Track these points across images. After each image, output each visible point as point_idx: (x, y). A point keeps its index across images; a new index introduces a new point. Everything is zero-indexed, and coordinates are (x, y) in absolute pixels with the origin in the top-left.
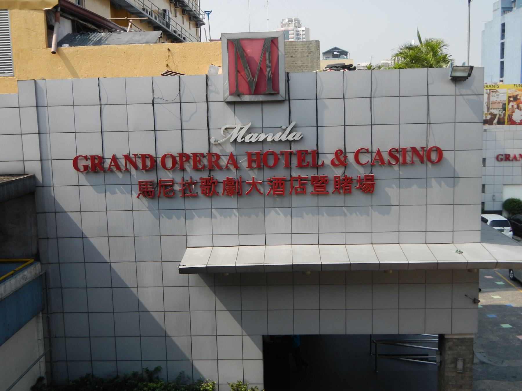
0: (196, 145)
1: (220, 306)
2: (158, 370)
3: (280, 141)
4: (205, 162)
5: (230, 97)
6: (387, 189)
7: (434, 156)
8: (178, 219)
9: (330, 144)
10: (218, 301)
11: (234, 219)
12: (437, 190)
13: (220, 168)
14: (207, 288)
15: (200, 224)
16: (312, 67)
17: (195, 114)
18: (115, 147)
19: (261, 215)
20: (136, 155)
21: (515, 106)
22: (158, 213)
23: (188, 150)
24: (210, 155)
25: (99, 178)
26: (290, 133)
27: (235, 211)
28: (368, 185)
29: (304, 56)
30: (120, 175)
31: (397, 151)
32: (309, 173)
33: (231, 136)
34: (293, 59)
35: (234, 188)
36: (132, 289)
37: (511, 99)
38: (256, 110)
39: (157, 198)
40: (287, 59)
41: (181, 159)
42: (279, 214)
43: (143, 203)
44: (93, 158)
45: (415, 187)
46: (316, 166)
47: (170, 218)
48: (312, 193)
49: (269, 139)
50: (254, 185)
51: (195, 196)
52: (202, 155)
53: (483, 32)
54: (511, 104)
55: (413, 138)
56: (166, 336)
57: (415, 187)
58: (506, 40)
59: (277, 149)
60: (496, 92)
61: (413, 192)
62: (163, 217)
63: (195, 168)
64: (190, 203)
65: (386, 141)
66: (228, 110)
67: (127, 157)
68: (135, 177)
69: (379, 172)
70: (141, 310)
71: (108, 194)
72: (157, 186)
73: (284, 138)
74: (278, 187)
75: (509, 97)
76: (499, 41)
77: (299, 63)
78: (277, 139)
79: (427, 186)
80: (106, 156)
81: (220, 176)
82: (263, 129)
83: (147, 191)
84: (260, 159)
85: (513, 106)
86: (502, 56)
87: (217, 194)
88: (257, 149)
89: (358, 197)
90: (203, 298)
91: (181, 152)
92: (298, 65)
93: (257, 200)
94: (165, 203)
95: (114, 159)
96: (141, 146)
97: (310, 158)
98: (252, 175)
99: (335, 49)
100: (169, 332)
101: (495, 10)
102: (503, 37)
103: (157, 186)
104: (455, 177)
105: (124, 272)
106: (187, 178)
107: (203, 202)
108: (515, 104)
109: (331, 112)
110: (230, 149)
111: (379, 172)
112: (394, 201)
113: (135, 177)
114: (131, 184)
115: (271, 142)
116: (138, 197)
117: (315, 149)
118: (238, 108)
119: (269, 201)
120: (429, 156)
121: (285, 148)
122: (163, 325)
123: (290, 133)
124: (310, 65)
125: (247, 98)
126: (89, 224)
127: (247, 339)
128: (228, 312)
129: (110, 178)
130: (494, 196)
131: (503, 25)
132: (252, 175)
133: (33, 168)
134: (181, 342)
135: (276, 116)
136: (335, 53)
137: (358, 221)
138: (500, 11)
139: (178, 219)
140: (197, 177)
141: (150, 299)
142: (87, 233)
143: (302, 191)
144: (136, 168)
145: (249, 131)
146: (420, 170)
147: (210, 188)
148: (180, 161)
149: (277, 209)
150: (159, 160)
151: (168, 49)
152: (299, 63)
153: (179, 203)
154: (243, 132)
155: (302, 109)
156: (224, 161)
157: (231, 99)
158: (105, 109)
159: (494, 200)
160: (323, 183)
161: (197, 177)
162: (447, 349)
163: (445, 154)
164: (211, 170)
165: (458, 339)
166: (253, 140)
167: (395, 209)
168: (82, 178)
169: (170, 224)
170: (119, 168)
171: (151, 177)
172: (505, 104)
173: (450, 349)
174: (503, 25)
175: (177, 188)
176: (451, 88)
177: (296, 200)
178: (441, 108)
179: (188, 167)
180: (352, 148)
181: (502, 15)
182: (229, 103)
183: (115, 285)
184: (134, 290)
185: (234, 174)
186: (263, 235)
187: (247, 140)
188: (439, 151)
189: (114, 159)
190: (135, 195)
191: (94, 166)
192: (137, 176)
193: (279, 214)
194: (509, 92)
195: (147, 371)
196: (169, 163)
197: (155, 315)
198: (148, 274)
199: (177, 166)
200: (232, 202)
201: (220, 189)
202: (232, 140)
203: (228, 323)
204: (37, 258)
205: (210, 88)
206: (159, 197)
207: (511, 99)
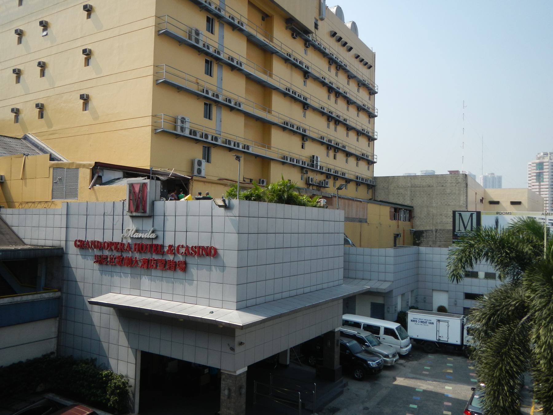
2: (96, 359)
3: (146, 238)
6: (192, 270)
7: (213, 252)
9: (169, 241)
12: (216, 273)
16: (459, 194)
19: (139, 278)
22: (102, 272)
24: (121, 244)
28: (183, 267)
29: (453, 186)
31: (195, 247)
34: (443, 188)
40: (439, 188)
43: (96, 266)
45: (205, 270)
46: (163, 254)
56: (100, 341)
57: (205, 270)
61: (204, 272)
65: (192, 242)
69: (190, 260)
70: (92, 325)
74: (148, 265)
77: (448, 191)
79: (210, 270)
84: (141, 247)
88: (138, 242)
89: (180, 274)
90: (114, 322)
92: (448, 192)
93: (138, 270)
97: (159, 249)
100: (102, 339)
104: (224, 267)
109: (170, 225)
111: (190, 260)
112: (195, 278)
120: (209, 252)
121: (149, 243)
124: (457, 192)
126: (78, 274)
127: (130, 349)
130: (456, 301)
133: (63, 244)
134: (105, 345)
135: (147, 225)
137: (179, 287)
146: (208, 260)
148: (111, 245)
152: (448, 191)
158: (88, 216)
163: (219, 251)
167: (195, 282)
169: (106, 278)
177: (154, 272)
178: (218, 224)
186: (137, 288)
188: (215, 250)
191: (82, 245)
192: (97, 252)
195: (92, 359)
197: (97, 328)
204: (60, 290)
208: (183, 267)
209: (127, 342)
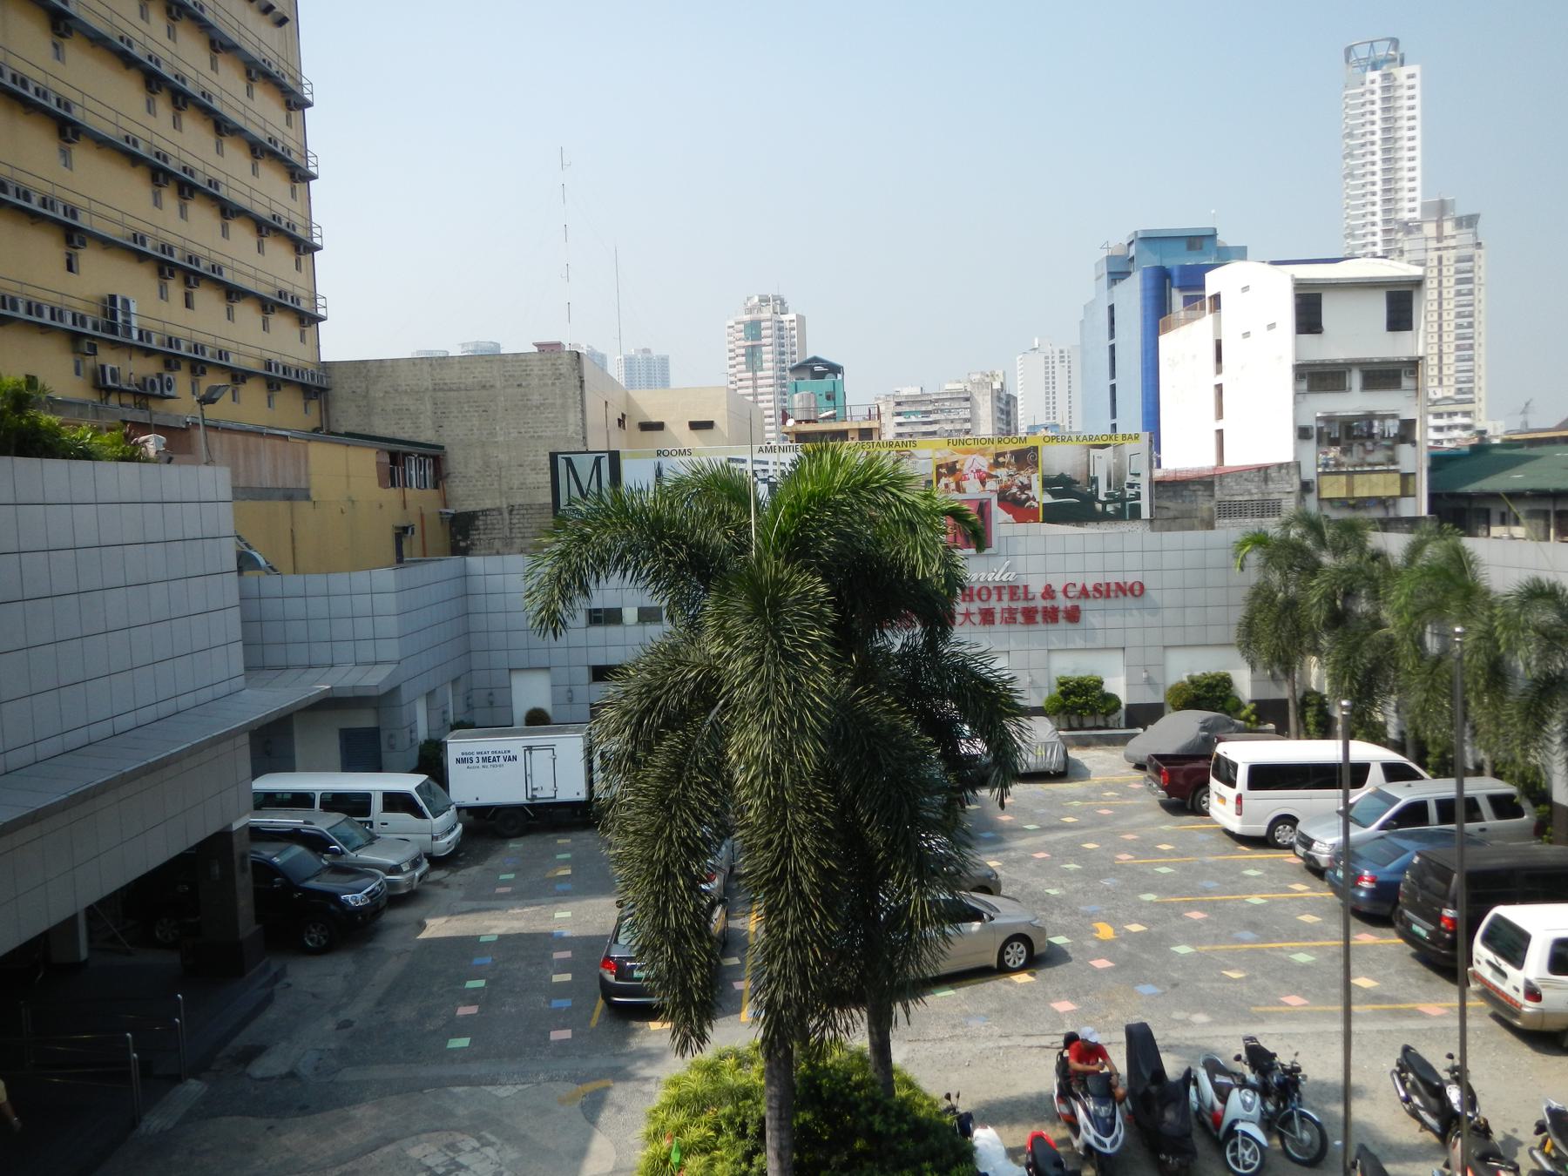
16: (563, 406)
21: (953, 486)
37: (943, 470)
53: (1082, 322)
54: (944, 481)
58: (1117, 341)
60: (911, 455)
75: (939, 467)
76: (1107, 343)
77: (536, 399)
85: (947, 486)
86: (1113, 376)
99: (816, 360)
101: (1098, 278)
102: (1112, 336)
108: (951, 481)
124: (559, 402)
131: (1112, 308)
136: (817, 369)
138: (1105, 278)
152: (536, 399)
159: (571, 700)
172: (931, 482)
174: (1112, 308)
181: (1110, 287)
194: (938, 455)
207: (943, 470)
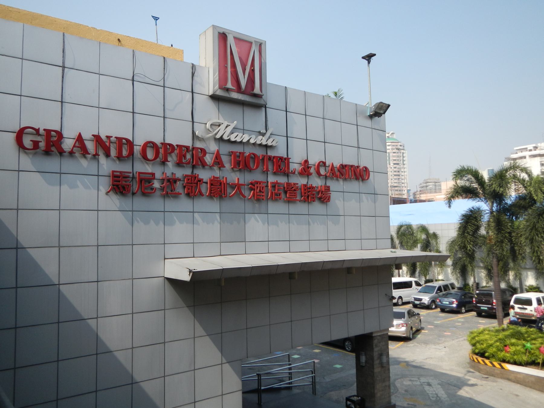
0: (179, 136)
1: (200, 331)
4: (189, 156)
5: (219, 90)
8: (157, 224)
10: (197, 325)
11: (217, 226)
13: (204, 165)
14: (186, 309)
15: (179, 230)
17: (180, 103)
18: (78, 125)
20: (108, 137)
23: (173, 139)
25: (52, 163)
26: (269, 138)
27: (218, 216)
28: (323, 196)
30: (84, 163)
32: (282, 180)
33: (216, 134)
35: (218, 190)
36: (89, 321)
38: (237, 111)
39: (130, 194)
41: (166, 150)
42: (258, 221)
43: (115, 201)
44: (48, 132)
46: (287, 174)
47: (147, 222)
48: (285, 202)
49: (252, 141)
50: (238, 187)
51: (176, 196)
52: (187, 148)
55: (350, 159)
56: (133, 383)
59: (260, 152)
62: (138, 222)
63: (179, 164)
64: (171, 204)
66: (212, 106)
67: (97, 138)
68: (105, 167)
70: (100, 351)
71: (65, 187)
72: (132, 180)
73: (264, 143)
78: (258, 142)
79: (360, 201)
80: (65, 134)
81: (204, 175)
82: (244, 131)
83: (120, 185)
87: (201, 194)
88: (238, 149)
89: (317, 207)
90: (181, 323)
91: (163, 142)
93: (237, 204)
94: (140, 202)
95: (80, 139)
96: (114, 127)
98: (233, 177)
103: (132, 180)
105: (79, 298)
106: (169, 174)
107: (184, 203)
110: (213, 147)
113: (105, 167)
114: (98, 175)
115: (253, 144)
116: (107, 193)
117: (286, 157)
118: (223, 106)
119: (249, 206)
122: (129, 368)
123: (269, 138)
125: (235, 95)
128: (207, 337)
129: (68, 164)
132: (233, 177)
135: (255, 120)
137: (319, 230)
139: (157, 224)
140: (180, 173)
141: (113, 333)
142: (23, 241)
143: (275, 197)
144: (108, 155)
145: (235, 129)
147: (193, 187)
148: (162, 151)
149: (256, 215)
150: (137, 149)
151: (119, 40)
153: (156, 203)
154: (229, 129)
155: (276, 118)
156: (209, 159)
157: (220, 93)
160: (295, 190)
161: (180, 173)
162: (374, 346)
164: (194, 167)
165: (380, 336)
166: (238, 139)
168: (26, 161)
169: (147, 230)
170: (84, 151)
171: (125, 167)
173: (376, 346)
175: (156, 184)
176: (368, 123)
177: (273, 207)
179: (172, 159)
180: (313, 160)
182: (214, 98)
183: (65, 317)
184: (92, 323)
185: (217, 173)
187: (233, 139)
189: (80, 139)
190: (103, 190)
192: (107, 166)
193: (258, 221)
196: (150, 154)
197: (120, 356)
198: (114, 297)
199: (158, 159)
200: (214, 205)
201: (204, 189)
202: (218, 136)
203: (208, 351)
205: (195, 78)
206: (133, 194)
208: (323, 196)
209: (218, 354)
